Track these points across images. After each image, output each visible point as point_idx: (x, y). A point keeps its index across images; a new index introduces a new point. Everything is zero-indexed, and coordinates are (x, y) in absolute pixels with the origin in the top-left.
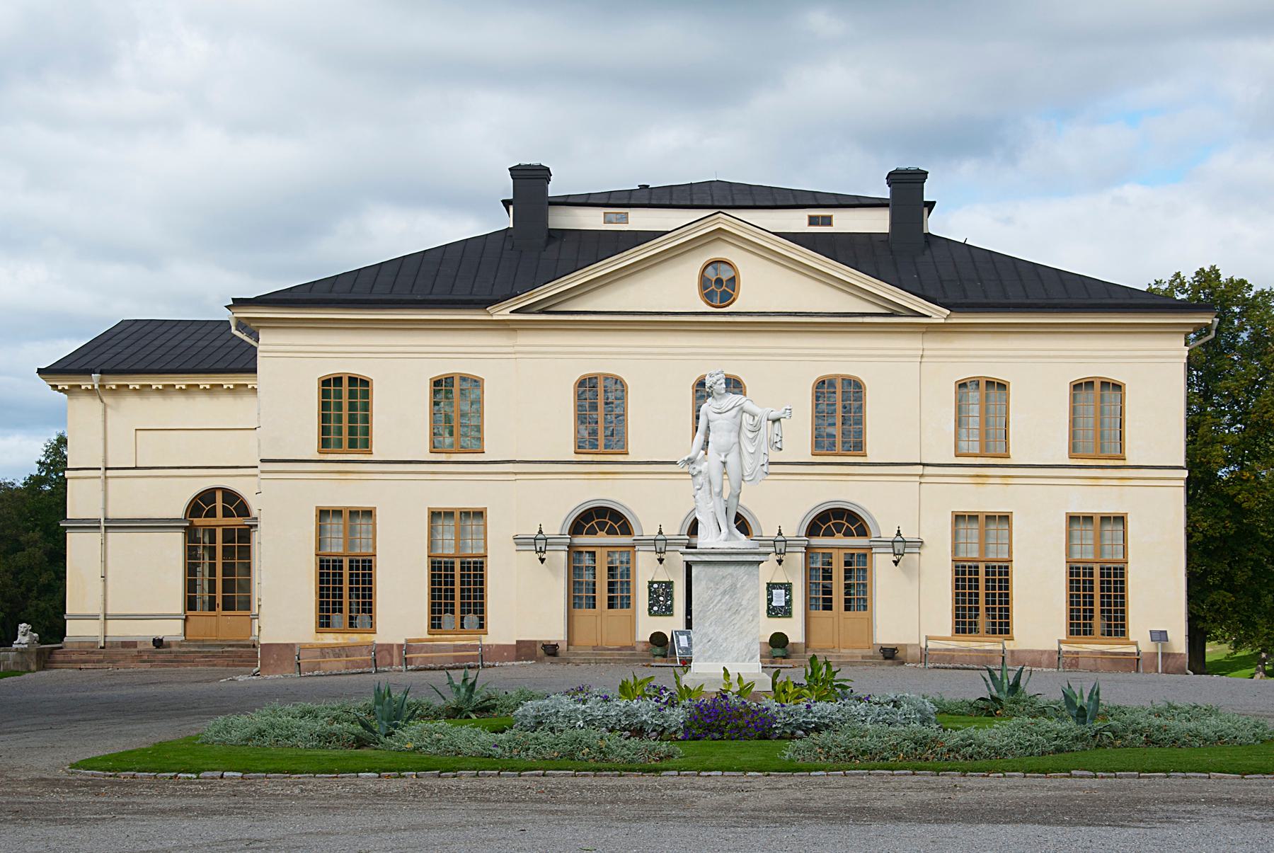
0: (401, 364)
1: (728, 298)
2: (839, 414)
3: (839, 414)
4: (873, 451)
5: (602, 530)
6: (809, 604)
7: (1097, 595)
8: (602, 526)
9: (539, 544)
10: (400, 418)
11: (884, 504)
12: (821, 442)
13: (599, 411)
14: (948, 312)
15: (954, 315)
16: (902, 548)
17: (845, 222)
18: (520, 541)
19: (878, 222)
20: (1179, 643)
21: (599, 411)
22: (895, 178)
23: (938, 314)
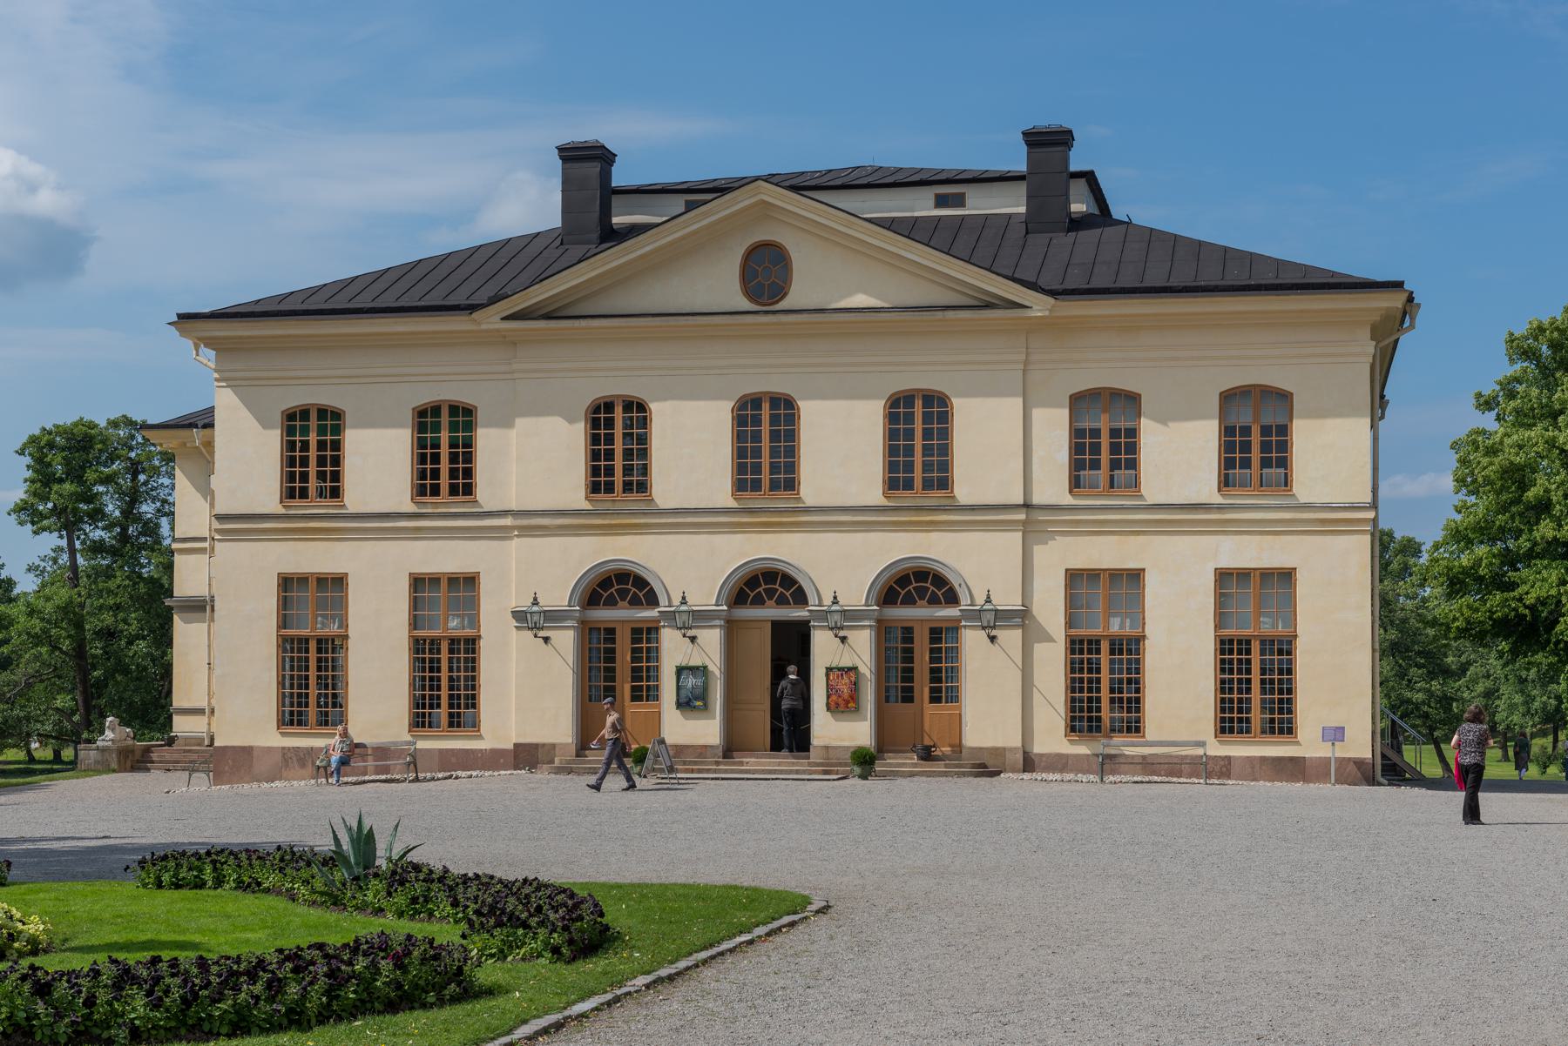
1: (780, 291)
2: (918, 445)
3: (918, 445)
4: (964, 491)
5: (623, 599)
6: (883, 698)
8: (623, 594)
9: (533, 620)
10: (378, 462)
11: (981, 563)
12: (897, 479)
14: (1050, 300)
15: (1059, 303)
16: (995, 620)
18: (519, 616)
19: (1012, 204)
20: (1360, 744)
21: (617, 450)
23: (1040, 306)
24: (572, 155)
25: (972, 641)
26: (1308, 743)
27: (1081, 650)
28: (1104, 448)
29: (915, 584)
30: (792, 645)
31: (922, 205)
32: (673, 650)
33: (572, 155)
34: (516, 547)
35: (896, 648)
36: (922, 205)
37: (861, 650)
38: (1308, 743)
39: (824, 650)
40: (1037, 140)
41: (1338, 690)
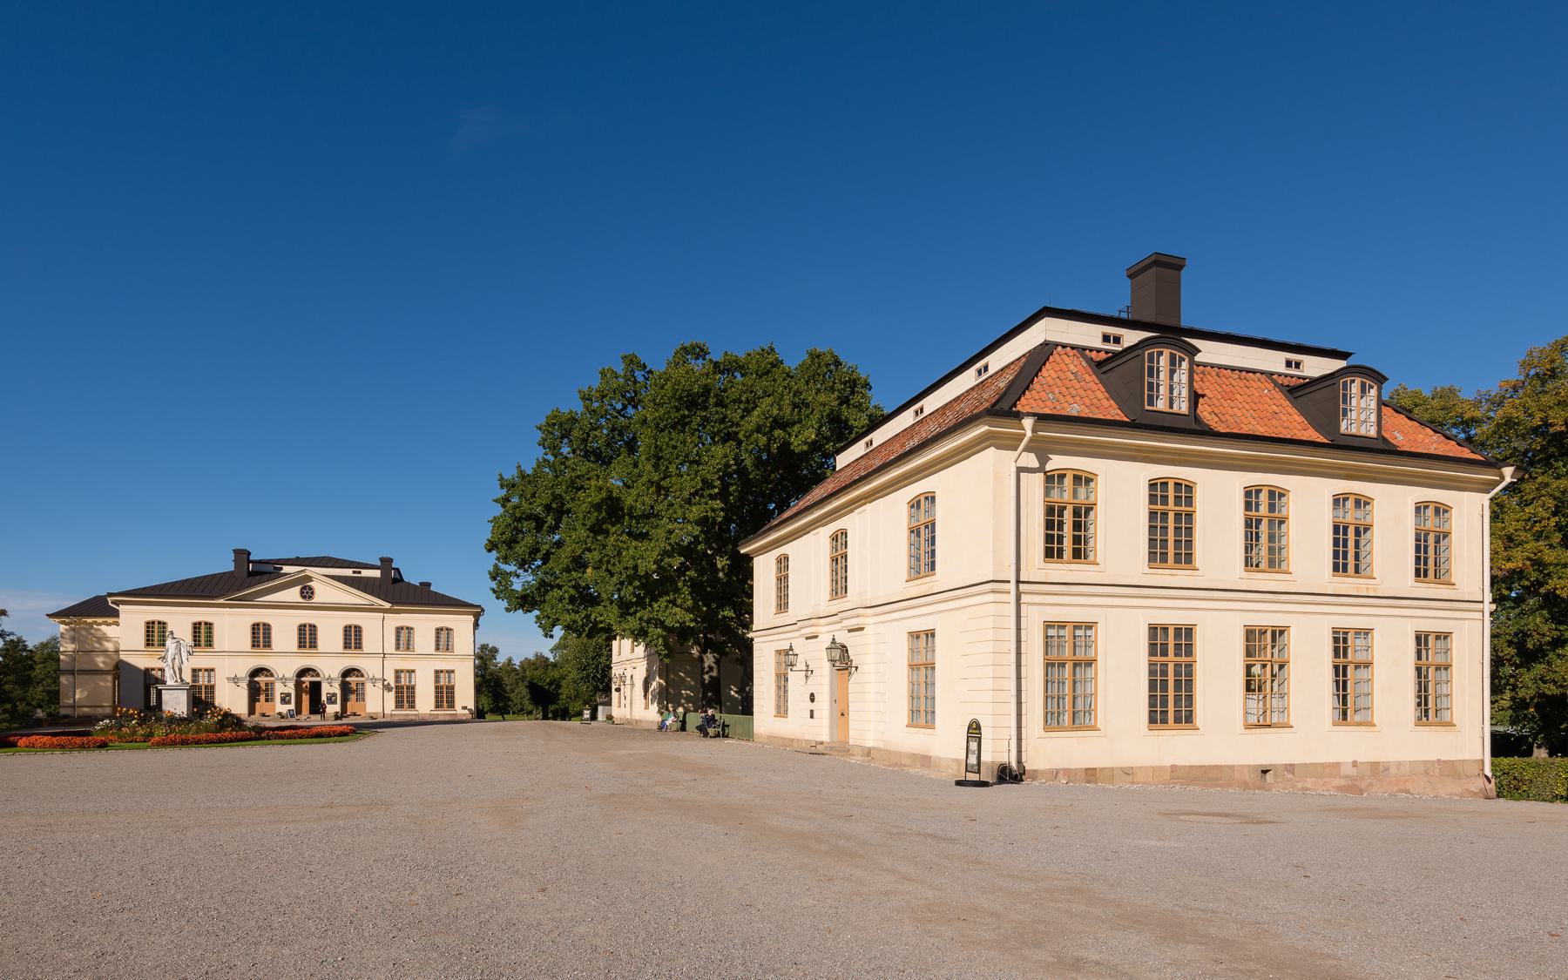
0: (180, 619)
2: (353, 637)
3: (353, 637)
7: (445, 695)
9: (235, 680)
11: (369, 666)
13: (261, 636)
16: (374, 680)
17: (366, 573)
19: (376, 573)
21: (261, 636)
22: (382, 560)
24: (237, 552)
25: (369, 686)
26: (459, 710)
27: (399, 689)
28: (404, 638)
29: (348, 673)
30: (315, 688)
31: (348, 572)
32: (279, 689)
33: (237, 552)
34: (227, 660)
35: (346, 689)
36: (348, 572)
37: (337, 690)
38: (459, 710)
39: (326, 689)
40: (382, 560)
41: (465, 697)
